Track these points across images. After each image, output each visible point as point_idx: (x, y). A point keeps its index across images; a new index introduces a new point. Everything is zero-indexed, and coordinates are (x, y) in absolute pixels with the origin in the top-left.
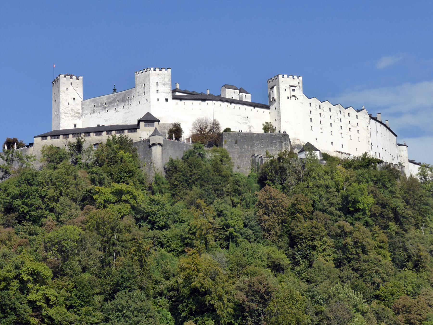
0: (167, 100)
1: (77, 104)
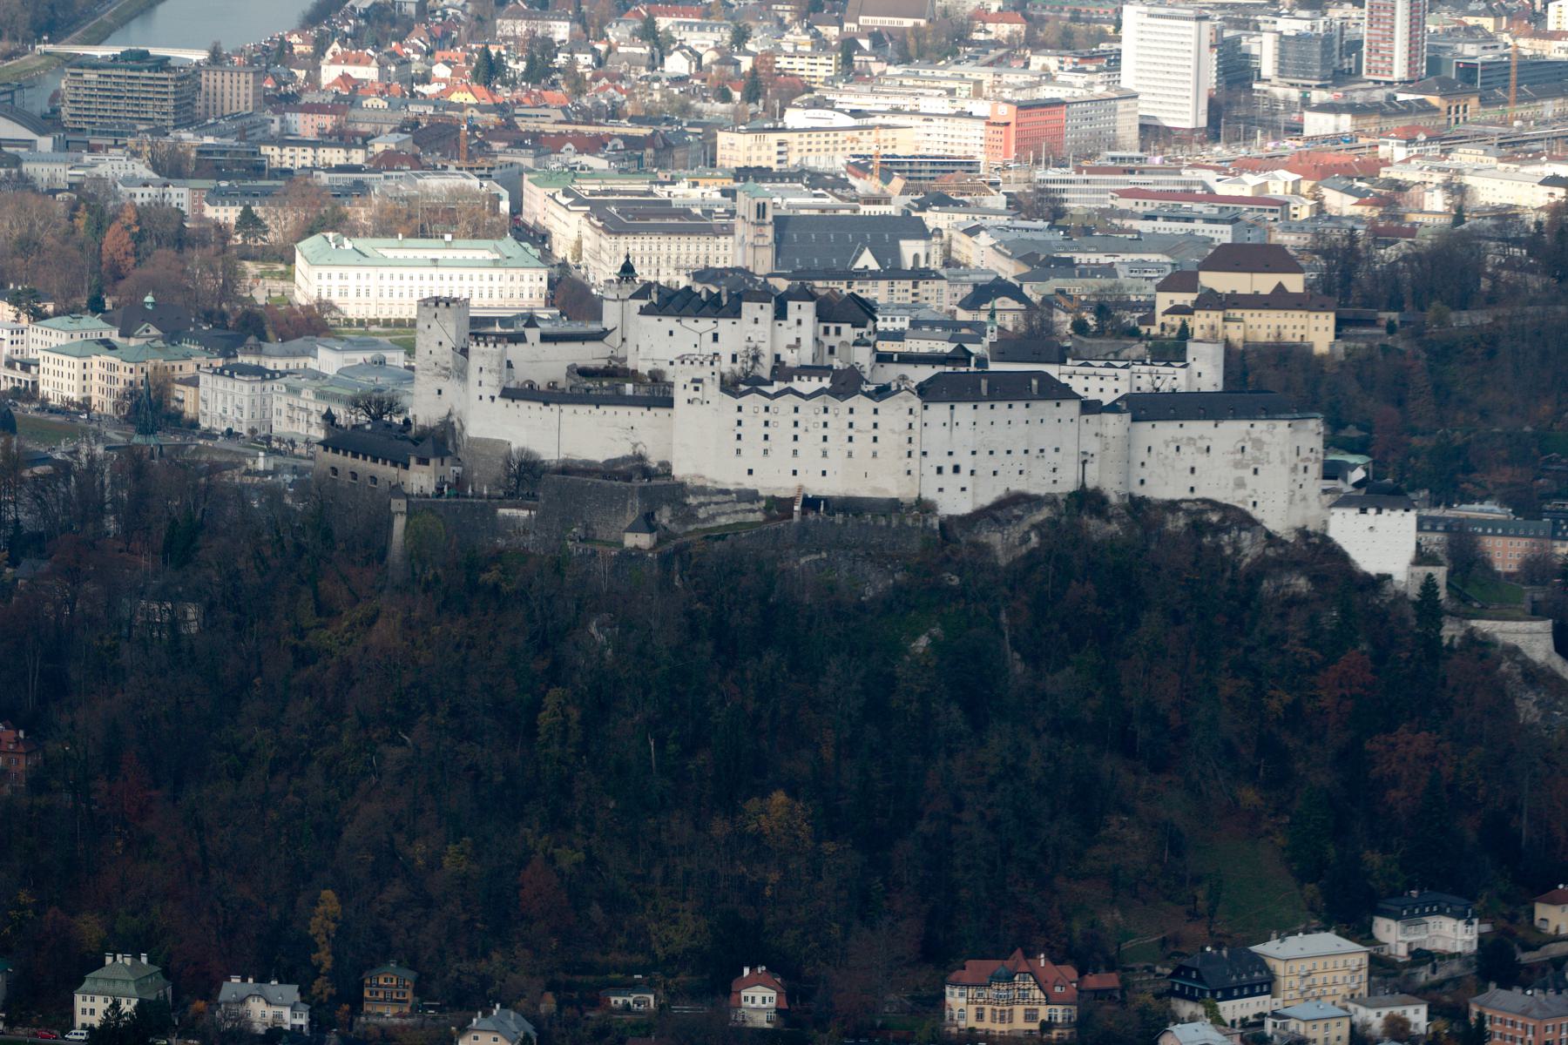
0: (493, 398)
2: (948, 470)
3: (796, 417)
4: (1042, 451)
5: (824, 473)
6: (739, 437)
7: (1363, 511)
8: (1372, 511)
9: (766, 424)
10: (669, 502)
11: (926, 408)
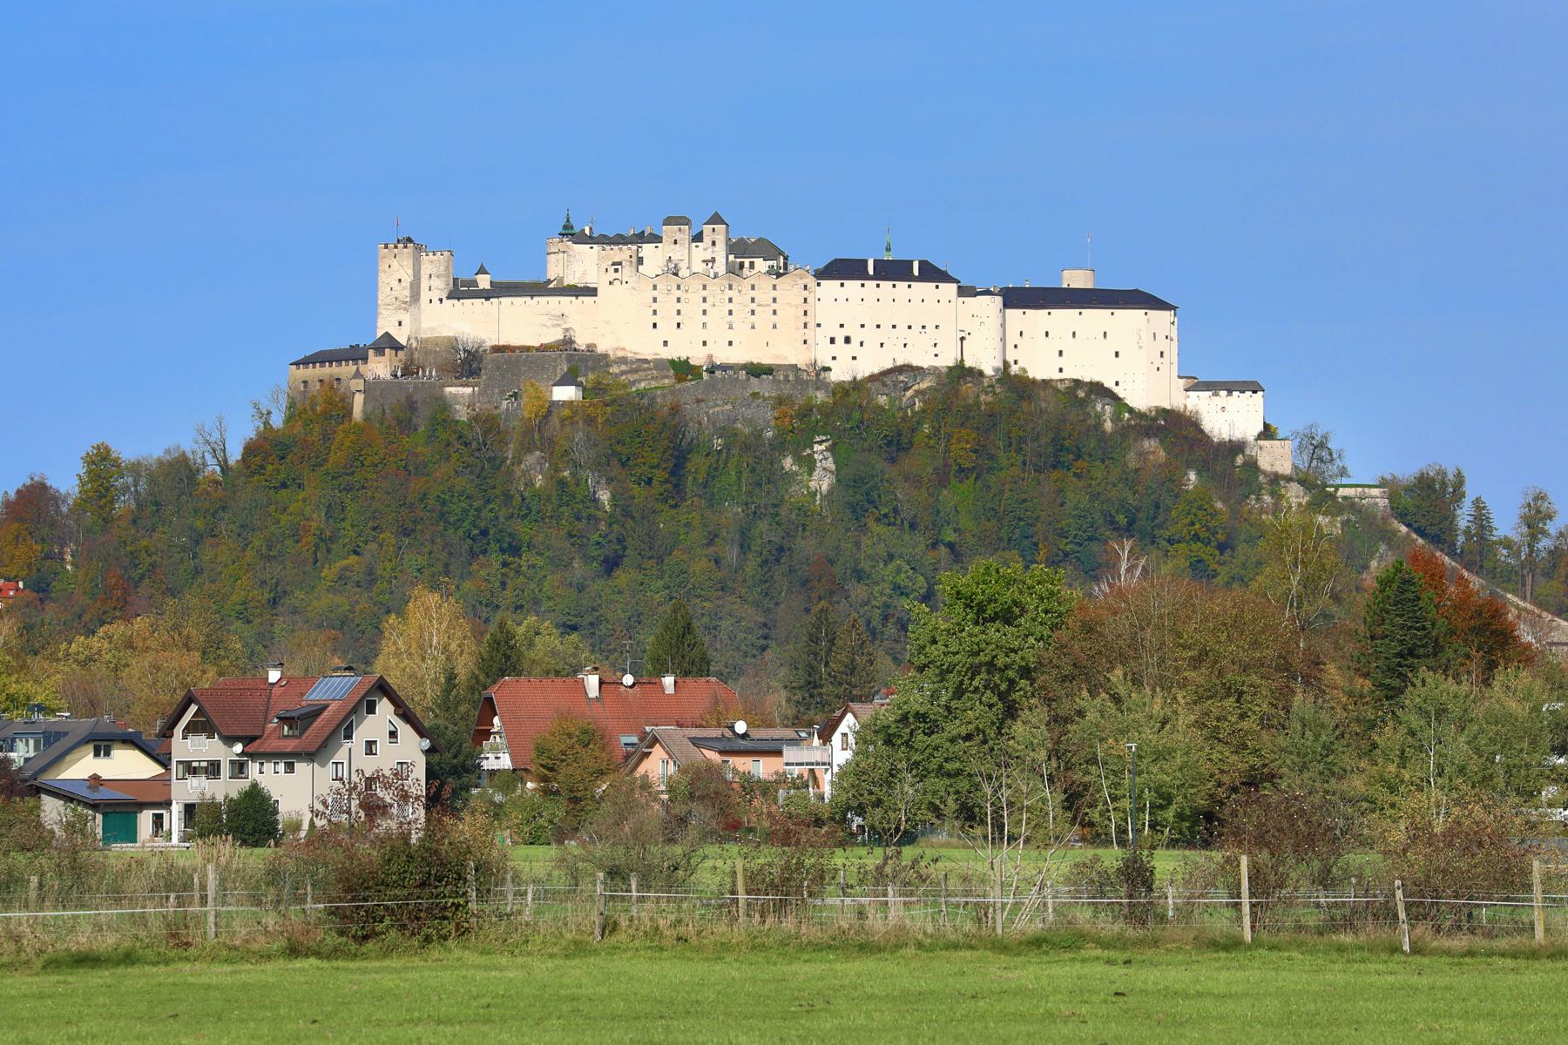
0: (441, 300)
1: (404, 288)
2: (840, 340)
3: (704, 293)
4: (923, 327)
5: (730, 343)
6: (655, 312)
7: (1216, 395)
8: (1223, 393)
9: (679, 300)
11: (819, 285)
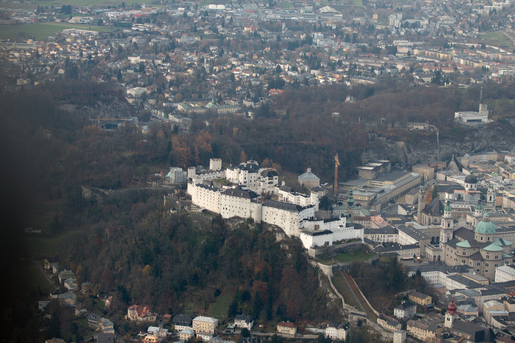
2: (225, 209)
10: (187, 205)
